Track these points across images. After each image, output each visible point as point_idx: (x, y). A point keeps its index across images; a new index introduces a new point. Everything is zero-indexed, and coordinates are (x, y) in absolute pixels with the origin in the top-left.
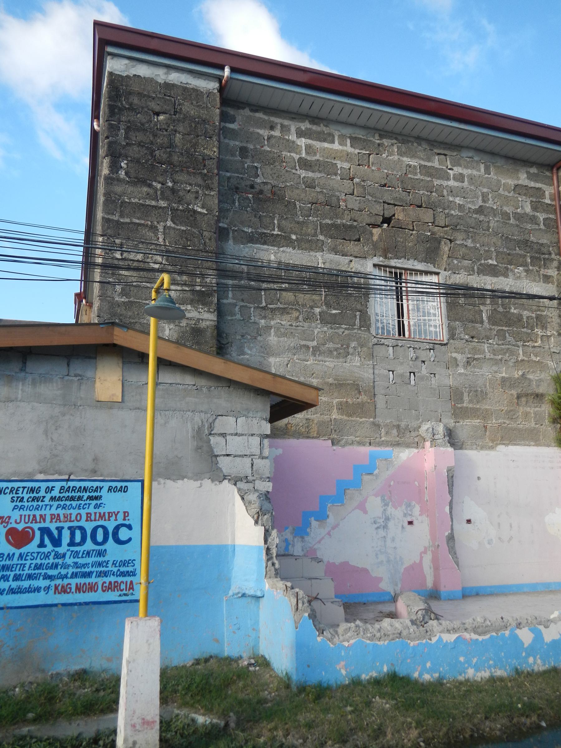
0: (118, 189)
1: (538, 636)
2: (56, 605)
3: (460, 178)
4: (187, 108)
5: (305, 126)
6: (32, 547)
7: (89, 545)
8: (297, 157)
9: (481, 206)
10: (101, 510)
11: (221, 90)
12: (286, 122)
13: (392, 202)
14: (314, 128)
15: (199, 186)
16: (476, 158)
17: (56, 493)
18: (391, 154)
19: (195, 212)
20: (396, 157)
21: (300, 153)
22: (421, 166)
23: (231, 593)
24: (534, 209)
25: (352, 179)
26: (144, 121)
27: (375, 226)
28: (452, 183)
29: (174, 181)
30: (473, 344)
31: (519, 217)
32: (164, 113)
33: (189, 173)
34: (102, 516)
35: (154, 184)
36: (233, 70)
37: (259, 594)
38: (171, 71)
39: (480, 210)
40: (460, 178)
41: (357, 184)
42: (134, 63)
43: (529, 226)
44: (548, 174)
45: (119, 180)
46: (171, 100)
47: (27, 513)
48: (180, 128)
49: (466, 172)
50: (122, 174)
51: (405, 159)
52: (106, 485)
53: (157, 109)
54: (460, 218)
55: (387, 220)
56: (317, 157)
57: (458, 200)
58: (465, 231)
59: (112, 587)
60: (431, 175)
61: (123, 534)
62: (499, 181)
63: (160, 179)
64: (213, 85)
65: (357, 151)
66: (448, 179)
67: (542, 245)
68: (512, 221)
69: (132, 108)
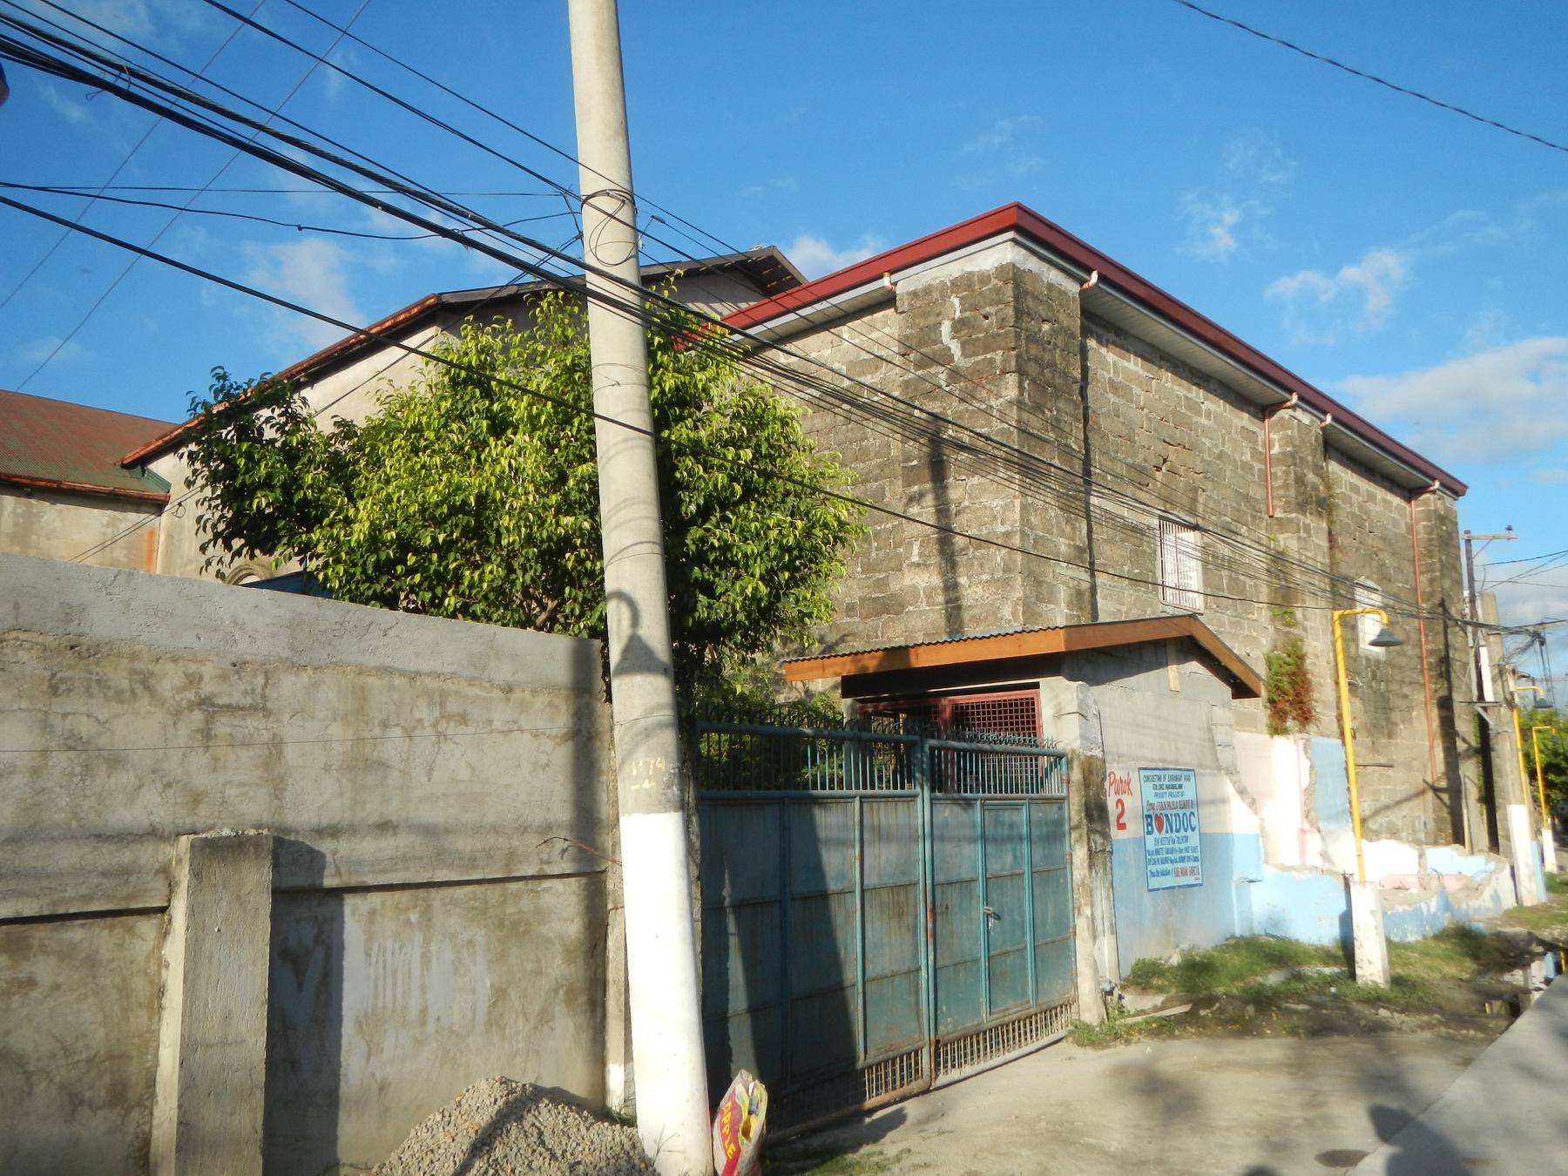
0: (1025, 416)
1: (1429, 910)
2: (1173, 888)
3: (1208, 415)
4: (1062, 317)
5: (1112, 336)
6: (1164, 834)
7: (1182, 833)
8: (1107, 376)
9: (1221, 451)
10: (1185, 798)
11: (1082, 293)
12: (1100, 331)
13: (1167, 440)
14: (1118, 340)
15: (1072, 416)
16: (1219, 392)
17: (1167, 782)
18: (1167, 381)
19: (1071, 448)
20: (1169, 385)
21: (1109, 372)
22: (1186, 397)
23: (1235, 878)
24: (1252, 457)
25: (1143, 409)
26: (1036, 329)
27: (1159, 469)
28: (1203, 421)
29: (1058, 411)
30: (1218, 614)
31: (1245, 465)
32: (1049, 321)
33: (1066, 399)
34: (1185, 805)
35: (1046, 411)
36: (1101, 278)
37: (1260, 878)
38: (1052, 268)
39: (1221, 455)
40: (1208, 414)
41: (1146, 415)
42: (1028, 253)
43: (1249, 478)
44: (1260, 415)
45: (1025, 404)
46: (1051, 305)
47: (1160, 800)
48: (1059, 343)
49: (1213, 407)
50: (1026, 395)
51: (1176, 388)
52: (1183, 773)
53: (1044, 314)
54: (1209, 463)
55: (1165, 461)
56: (1120, 379)
57: (1207, 442)
58: (1213, 480)
59: (1193, 871)
60: (1190, 410)
61: (1194, 822)
62: (1231, 421)
63: (1049, 407)
64: (1073, 288)
65: (1146, 374)
66: (1201, 416)
67: (1257, 500)
68: (1239, 471)
69: (1028, 314)
